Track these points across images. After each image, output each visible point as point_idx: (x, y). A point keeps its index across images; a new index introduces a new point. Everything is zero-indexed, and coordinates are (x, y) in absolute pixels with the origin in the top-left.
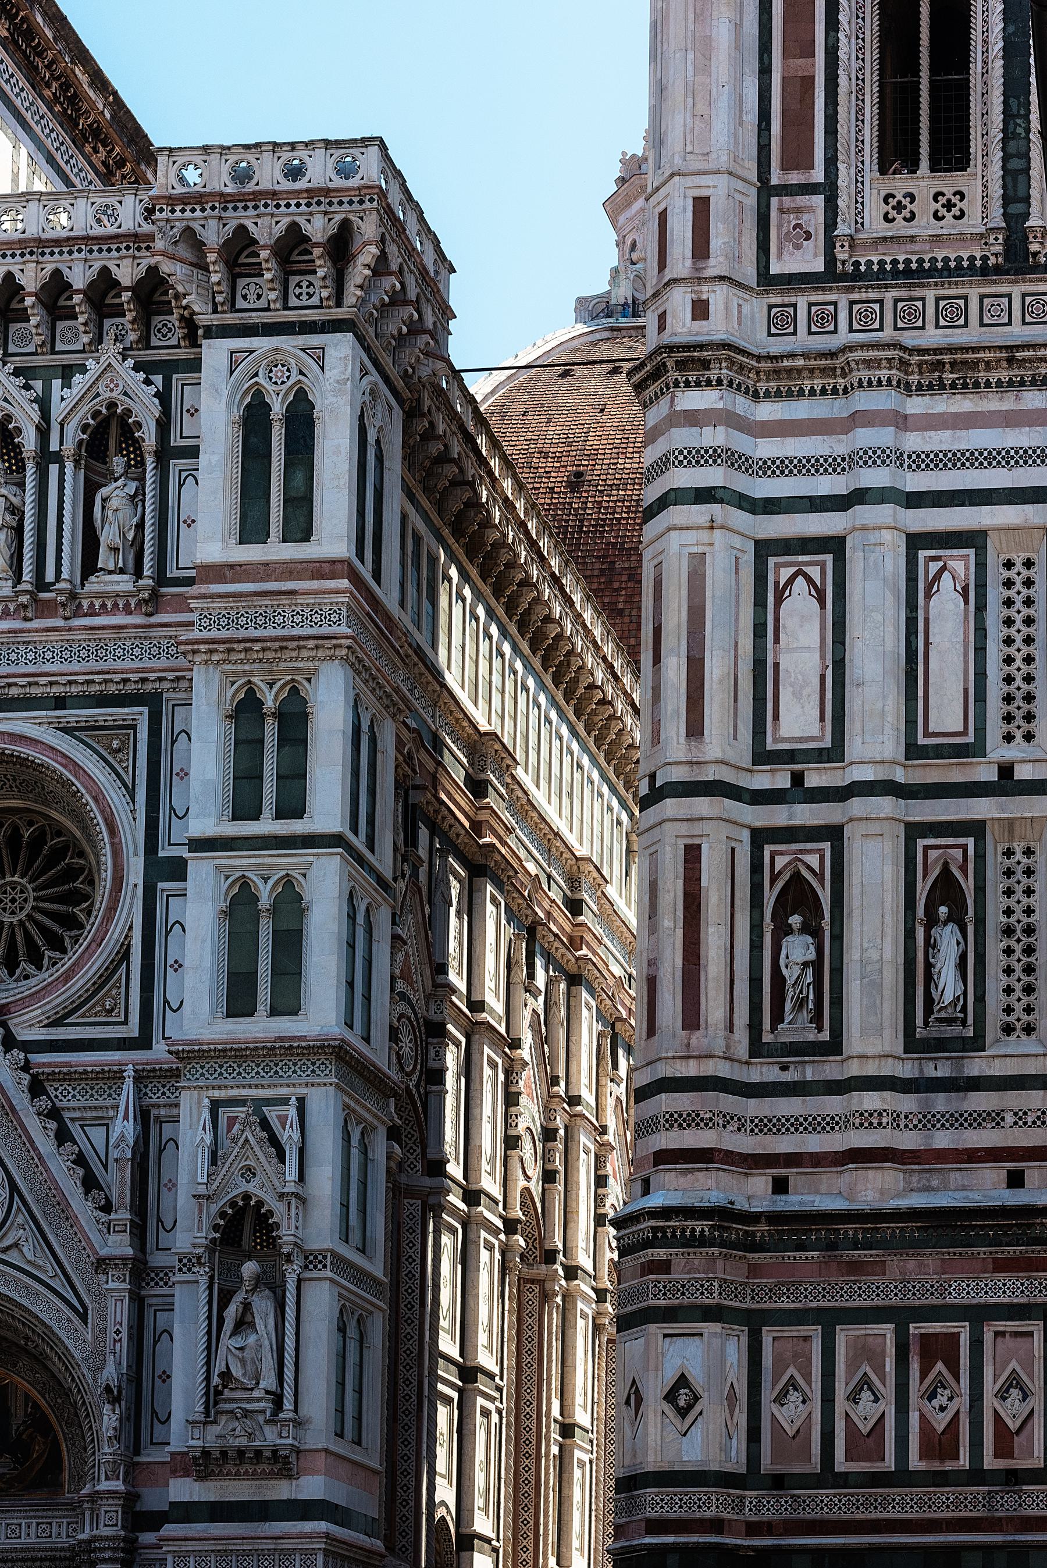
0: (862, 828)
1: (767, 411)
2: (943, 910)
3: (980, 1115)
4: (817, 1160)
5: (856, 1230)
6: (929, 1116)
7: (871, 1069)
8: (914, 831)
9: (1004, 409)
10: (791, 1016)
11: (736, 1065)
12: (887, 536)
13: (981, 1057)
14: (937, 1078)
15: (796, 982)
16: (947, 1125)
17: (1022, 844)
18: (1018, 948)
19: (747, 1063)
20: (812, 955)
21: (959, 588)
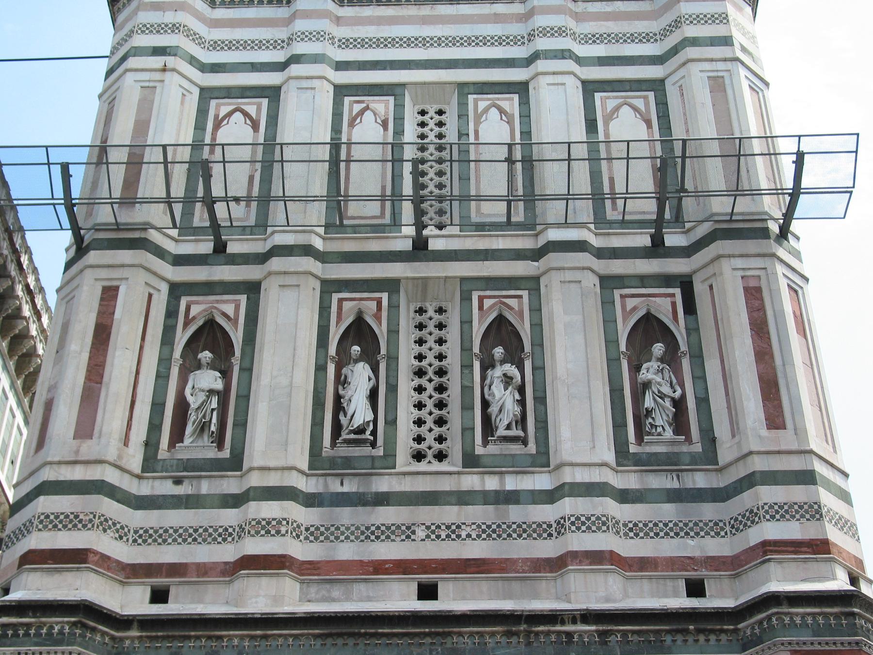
0: (281, 280)
1: (221, 13)
2: (356, 349)
3: (388, 528)
4: (204, 570)
5: (242, 637)
6: (333, 529)
7: (273, 480)
8: (329, 287)
9: (422, 14)
10: (191, 440)
11: (127, 476)
12: (316, 83)
13: (390, 474)
14: (343, 494)
15: (199, 408)
16: (352, 538)
17: (434, 304)
18: (430, 387)
19: (139, 477)
20: (219, 385)
21: (379, 121)
